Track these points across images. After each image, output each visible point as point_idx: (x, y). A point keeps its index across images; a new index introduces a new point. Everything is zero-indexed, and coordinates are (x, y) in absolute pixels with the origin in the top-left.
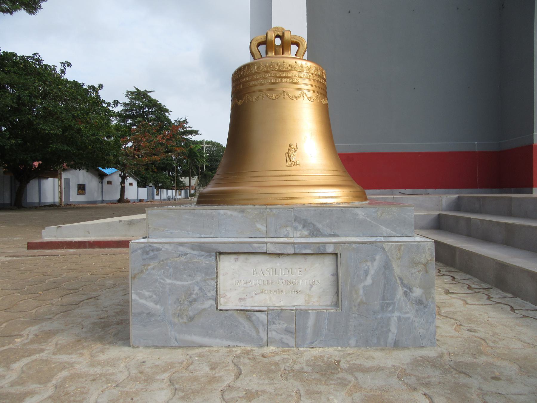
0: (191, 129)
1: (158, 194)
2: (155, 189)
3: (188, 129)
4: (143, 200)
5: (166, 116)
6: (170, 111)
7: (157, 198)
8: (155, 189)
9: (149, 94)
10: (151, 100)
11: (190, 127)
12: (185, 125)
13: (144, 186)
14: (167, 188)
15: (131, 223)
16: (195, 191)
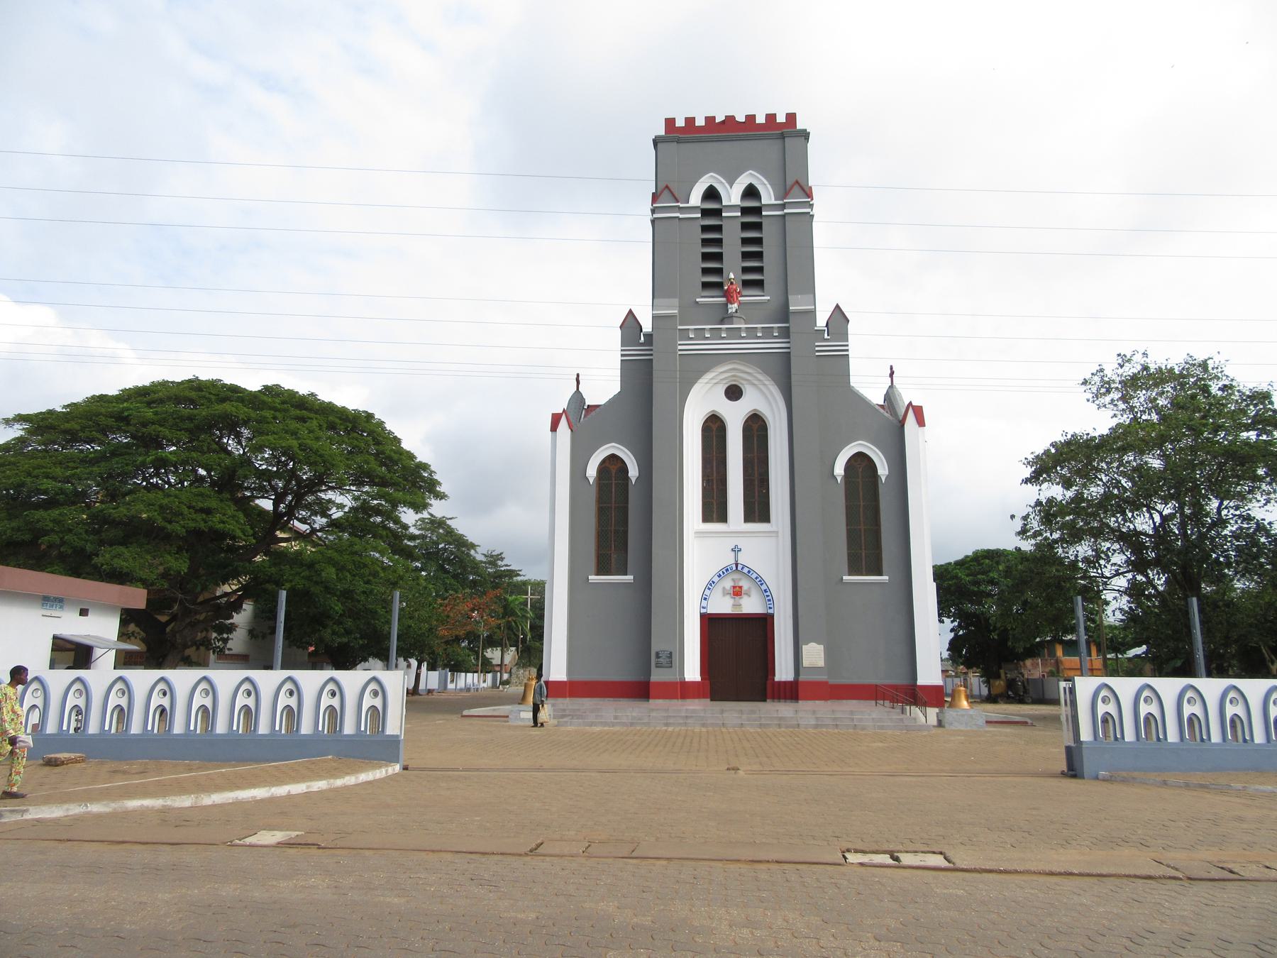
0: (508, 568)
1: (452, 681)
2: (449, 673)
3: (503, 569)
4: (434, 690)
5: (471, 556)
6: (477, 546)
7: (451, 686)
8: (449, 673)
9: (449, 522)
10: (450, 532)
11: (507, 565)
12: (500, 563)
13: (435, 670)
14: (467, 671)
15: (494, 710)
16: (511, 675)
